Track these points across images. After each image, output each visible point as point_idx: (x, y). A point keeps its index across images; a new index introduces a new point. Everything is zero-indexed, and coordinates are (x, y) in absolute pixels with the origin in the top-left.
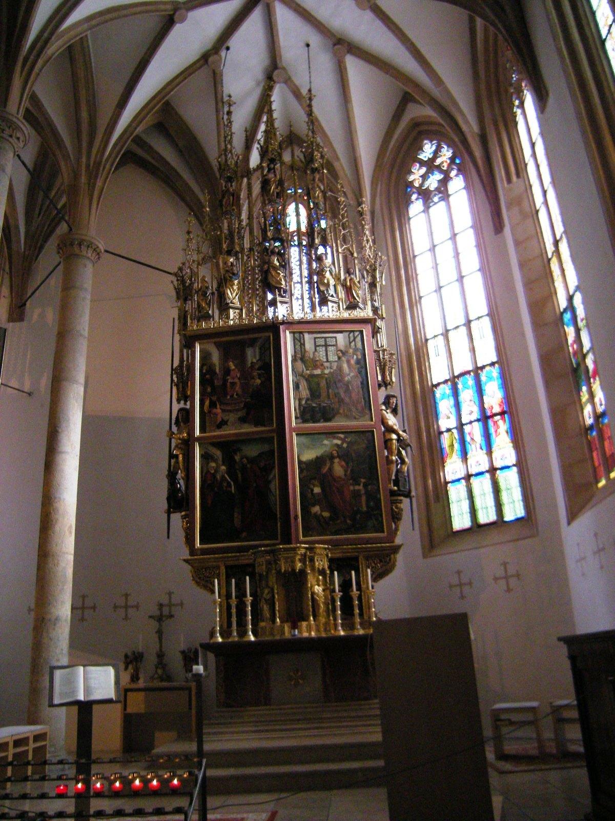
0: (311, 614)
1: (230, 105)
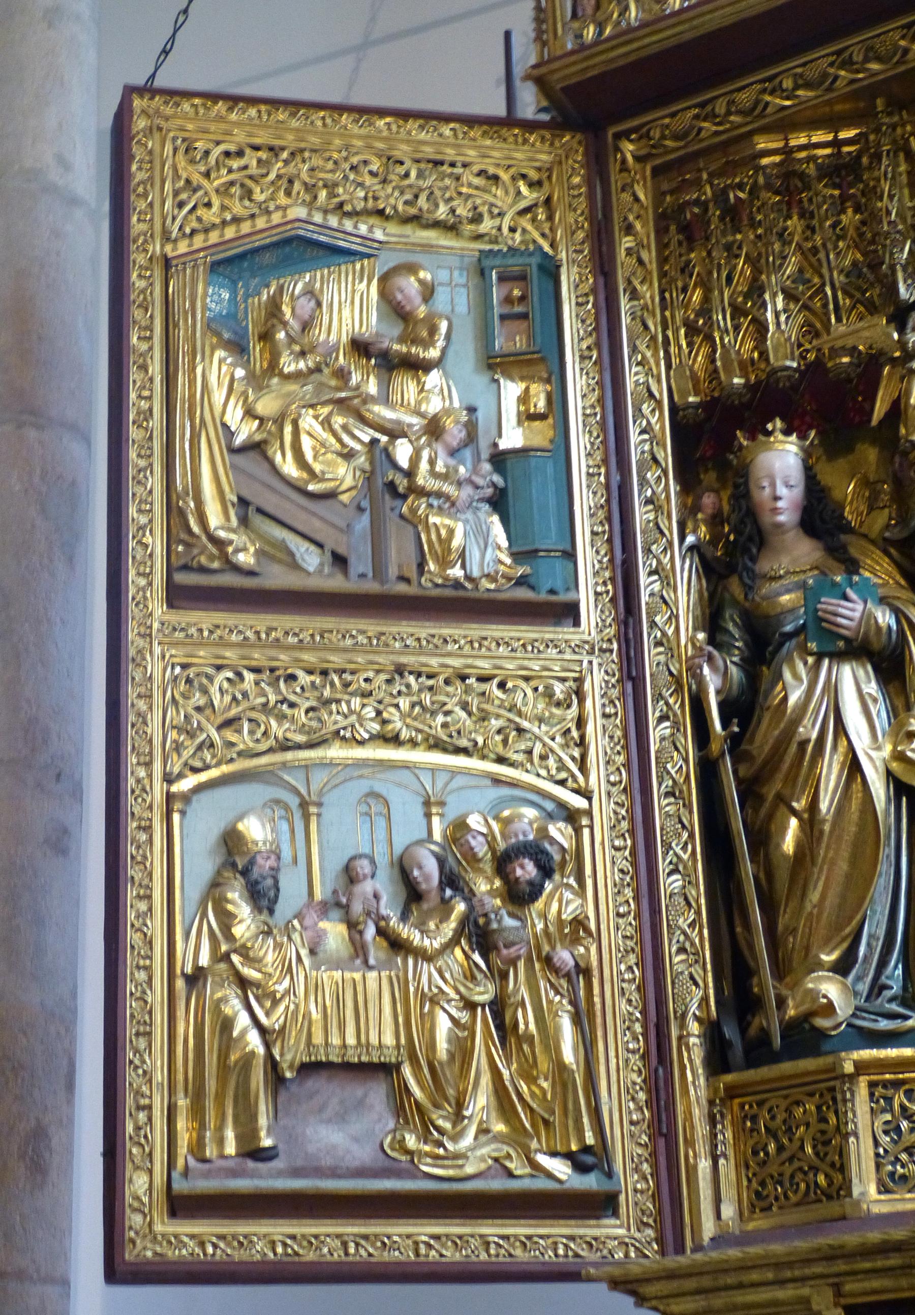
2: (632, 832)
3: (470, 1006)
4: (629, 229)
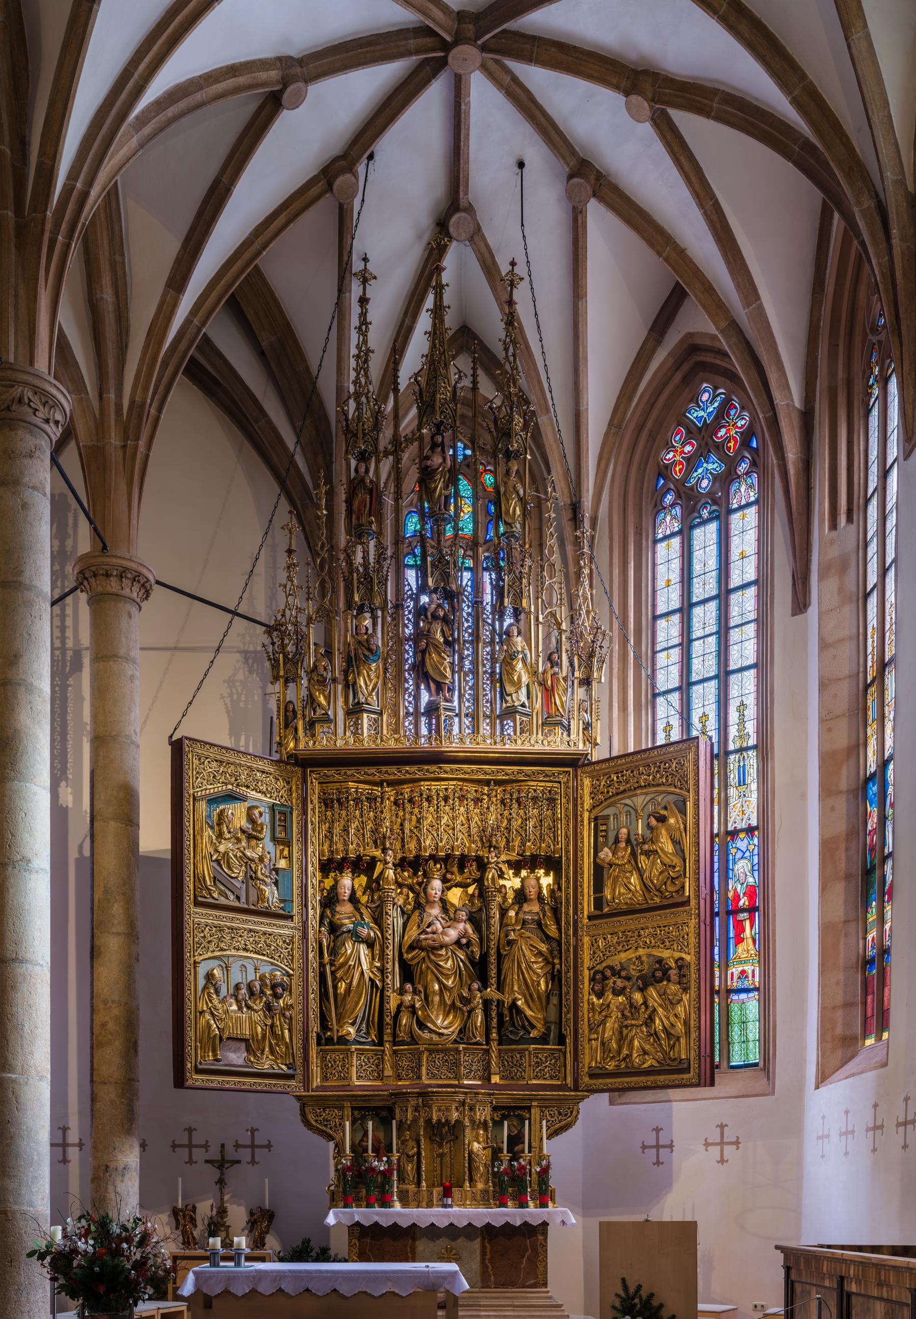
0: (467, 1178)
1: (365, 281)
3: (266, 1025)
4: (312, 801)
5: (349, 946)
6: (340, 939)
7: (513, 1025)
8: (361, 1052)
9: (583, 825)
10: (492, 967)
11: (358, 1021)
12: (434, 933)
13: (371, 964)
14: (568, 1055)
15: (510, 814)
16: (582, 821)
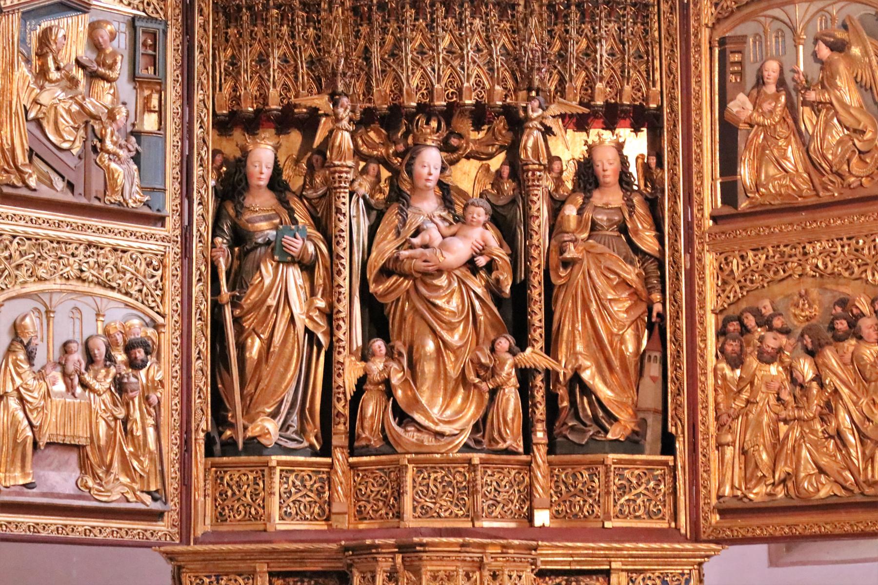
2: (181, 336)
4: (201, 11)
5: (267, 270)
6: (251, 256)
7: (577, 416)
8: (289, 468)
9: (699, 52)
10: (536, 308)
11: (284, 409)
12: (426, 246)
13: (310, 304)
14: (680, 472)
15: (567, 31)
16: (699, 45)
